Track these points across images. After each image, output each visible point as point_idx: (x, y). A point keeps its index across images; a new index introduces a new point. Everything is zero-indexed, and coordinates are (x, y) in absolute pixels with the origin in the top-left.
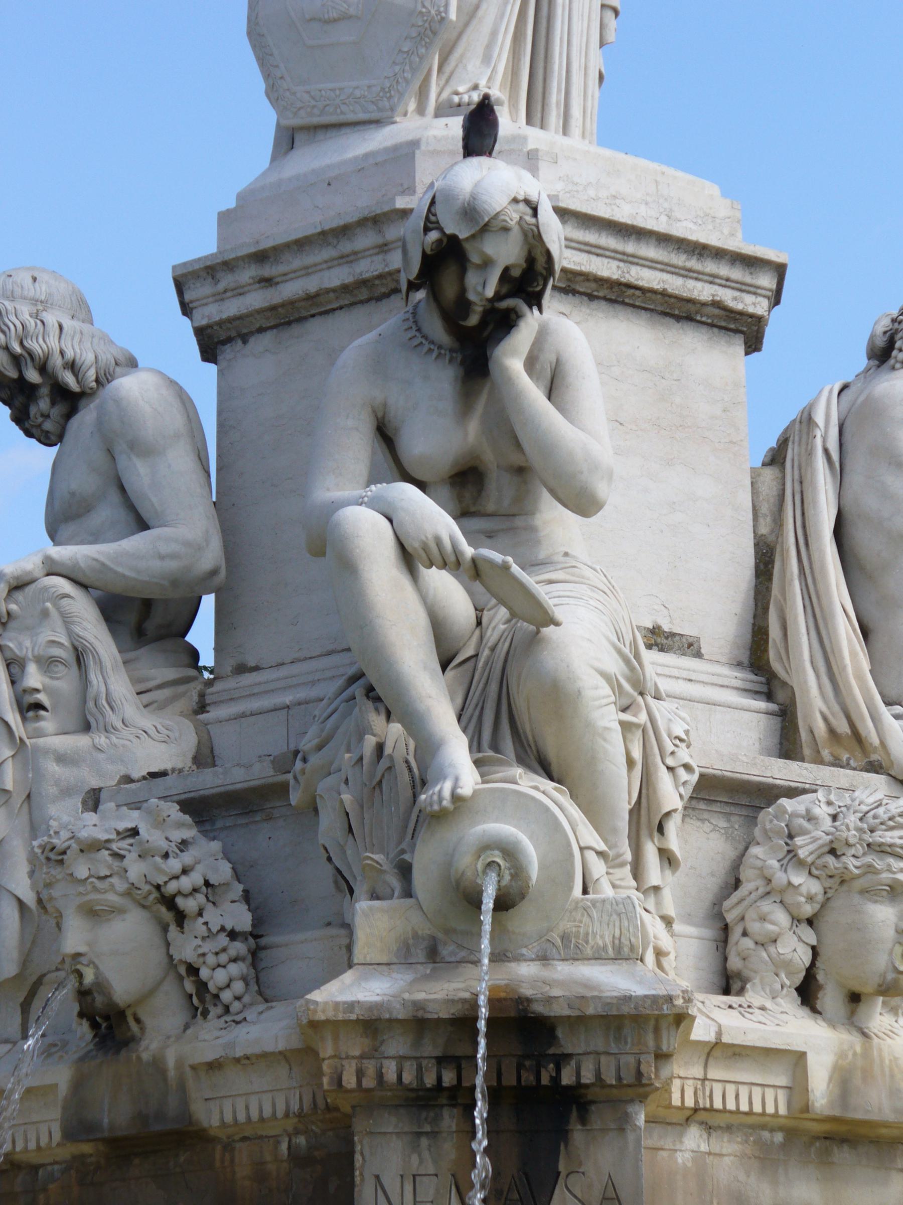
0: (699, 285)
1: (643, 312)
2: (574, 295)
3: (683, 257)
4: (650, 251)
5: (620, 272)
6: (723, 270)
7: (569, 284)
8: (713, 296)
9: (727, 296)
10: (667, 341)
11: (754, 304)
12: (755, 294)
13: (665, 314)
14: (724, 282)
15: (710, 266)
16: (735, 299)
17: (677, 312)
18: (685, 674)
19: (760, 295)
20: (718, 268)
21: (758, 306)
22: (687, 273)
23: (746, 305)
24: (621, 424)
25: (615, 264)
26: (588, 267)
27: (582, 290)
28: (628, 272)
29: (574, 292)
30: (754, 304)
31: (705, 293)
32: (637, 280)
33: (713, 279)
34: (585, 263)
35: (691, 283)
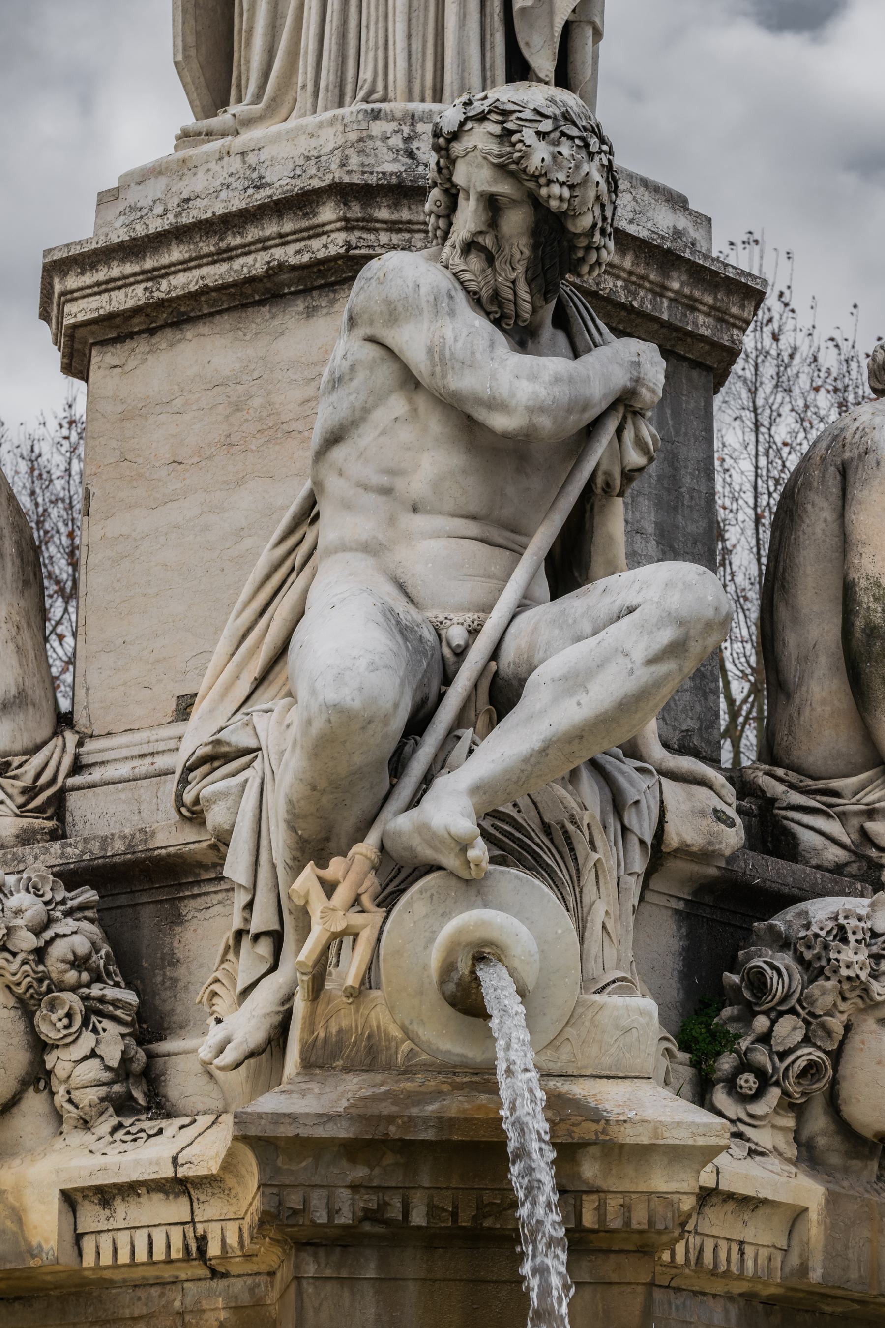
0: (250, 259)
1: (218, 317)
2: (132, 338)
3: (214, 240)
4: (177, 253)
5: (148, 294)
6: (271, 229)
7: (118, 330)
8: (269, 263)
9: (287, 254)
10: (247, 338)
11: (325, 247)
12: (324, 233)
13: (244, 306)
14: (277, 241)
15: (253, 233)
16: (298, 252)
17: (257, 298)
18: (136, 751)
19: (332, 231)
20: (263, 229)
21: (331, 246)
22: (224, 255)
23: (313, 253)
24: (180, 463)
25: (139, 289)
26: (108, 308)
27: (136, 329)
28: (158, 289)
29: (131, 335)
30: (325, 247)
31: (257, 265)
32: (169, 293)
33: (263, 244)
34: (104, 304)
35: (237, 264)
